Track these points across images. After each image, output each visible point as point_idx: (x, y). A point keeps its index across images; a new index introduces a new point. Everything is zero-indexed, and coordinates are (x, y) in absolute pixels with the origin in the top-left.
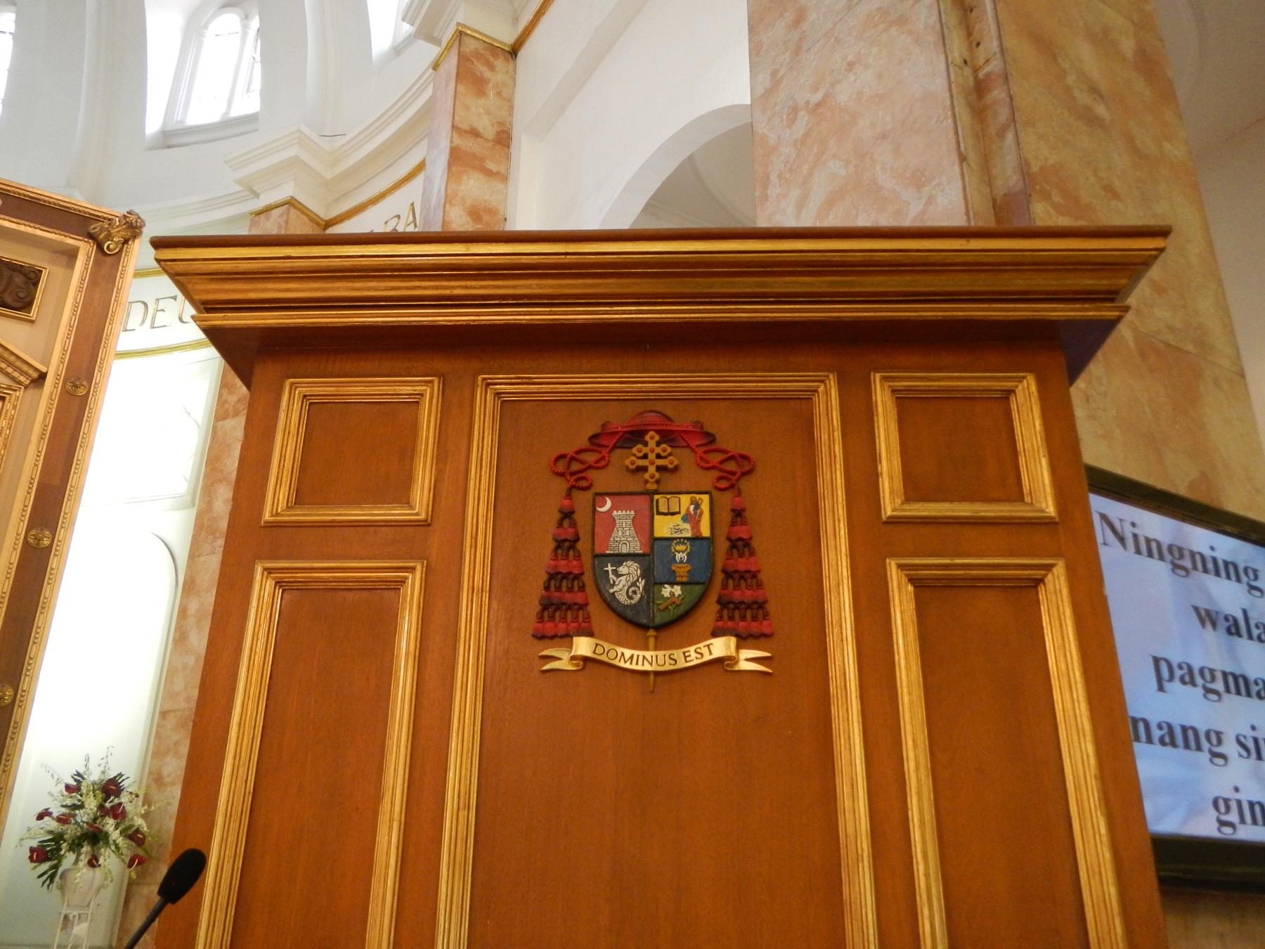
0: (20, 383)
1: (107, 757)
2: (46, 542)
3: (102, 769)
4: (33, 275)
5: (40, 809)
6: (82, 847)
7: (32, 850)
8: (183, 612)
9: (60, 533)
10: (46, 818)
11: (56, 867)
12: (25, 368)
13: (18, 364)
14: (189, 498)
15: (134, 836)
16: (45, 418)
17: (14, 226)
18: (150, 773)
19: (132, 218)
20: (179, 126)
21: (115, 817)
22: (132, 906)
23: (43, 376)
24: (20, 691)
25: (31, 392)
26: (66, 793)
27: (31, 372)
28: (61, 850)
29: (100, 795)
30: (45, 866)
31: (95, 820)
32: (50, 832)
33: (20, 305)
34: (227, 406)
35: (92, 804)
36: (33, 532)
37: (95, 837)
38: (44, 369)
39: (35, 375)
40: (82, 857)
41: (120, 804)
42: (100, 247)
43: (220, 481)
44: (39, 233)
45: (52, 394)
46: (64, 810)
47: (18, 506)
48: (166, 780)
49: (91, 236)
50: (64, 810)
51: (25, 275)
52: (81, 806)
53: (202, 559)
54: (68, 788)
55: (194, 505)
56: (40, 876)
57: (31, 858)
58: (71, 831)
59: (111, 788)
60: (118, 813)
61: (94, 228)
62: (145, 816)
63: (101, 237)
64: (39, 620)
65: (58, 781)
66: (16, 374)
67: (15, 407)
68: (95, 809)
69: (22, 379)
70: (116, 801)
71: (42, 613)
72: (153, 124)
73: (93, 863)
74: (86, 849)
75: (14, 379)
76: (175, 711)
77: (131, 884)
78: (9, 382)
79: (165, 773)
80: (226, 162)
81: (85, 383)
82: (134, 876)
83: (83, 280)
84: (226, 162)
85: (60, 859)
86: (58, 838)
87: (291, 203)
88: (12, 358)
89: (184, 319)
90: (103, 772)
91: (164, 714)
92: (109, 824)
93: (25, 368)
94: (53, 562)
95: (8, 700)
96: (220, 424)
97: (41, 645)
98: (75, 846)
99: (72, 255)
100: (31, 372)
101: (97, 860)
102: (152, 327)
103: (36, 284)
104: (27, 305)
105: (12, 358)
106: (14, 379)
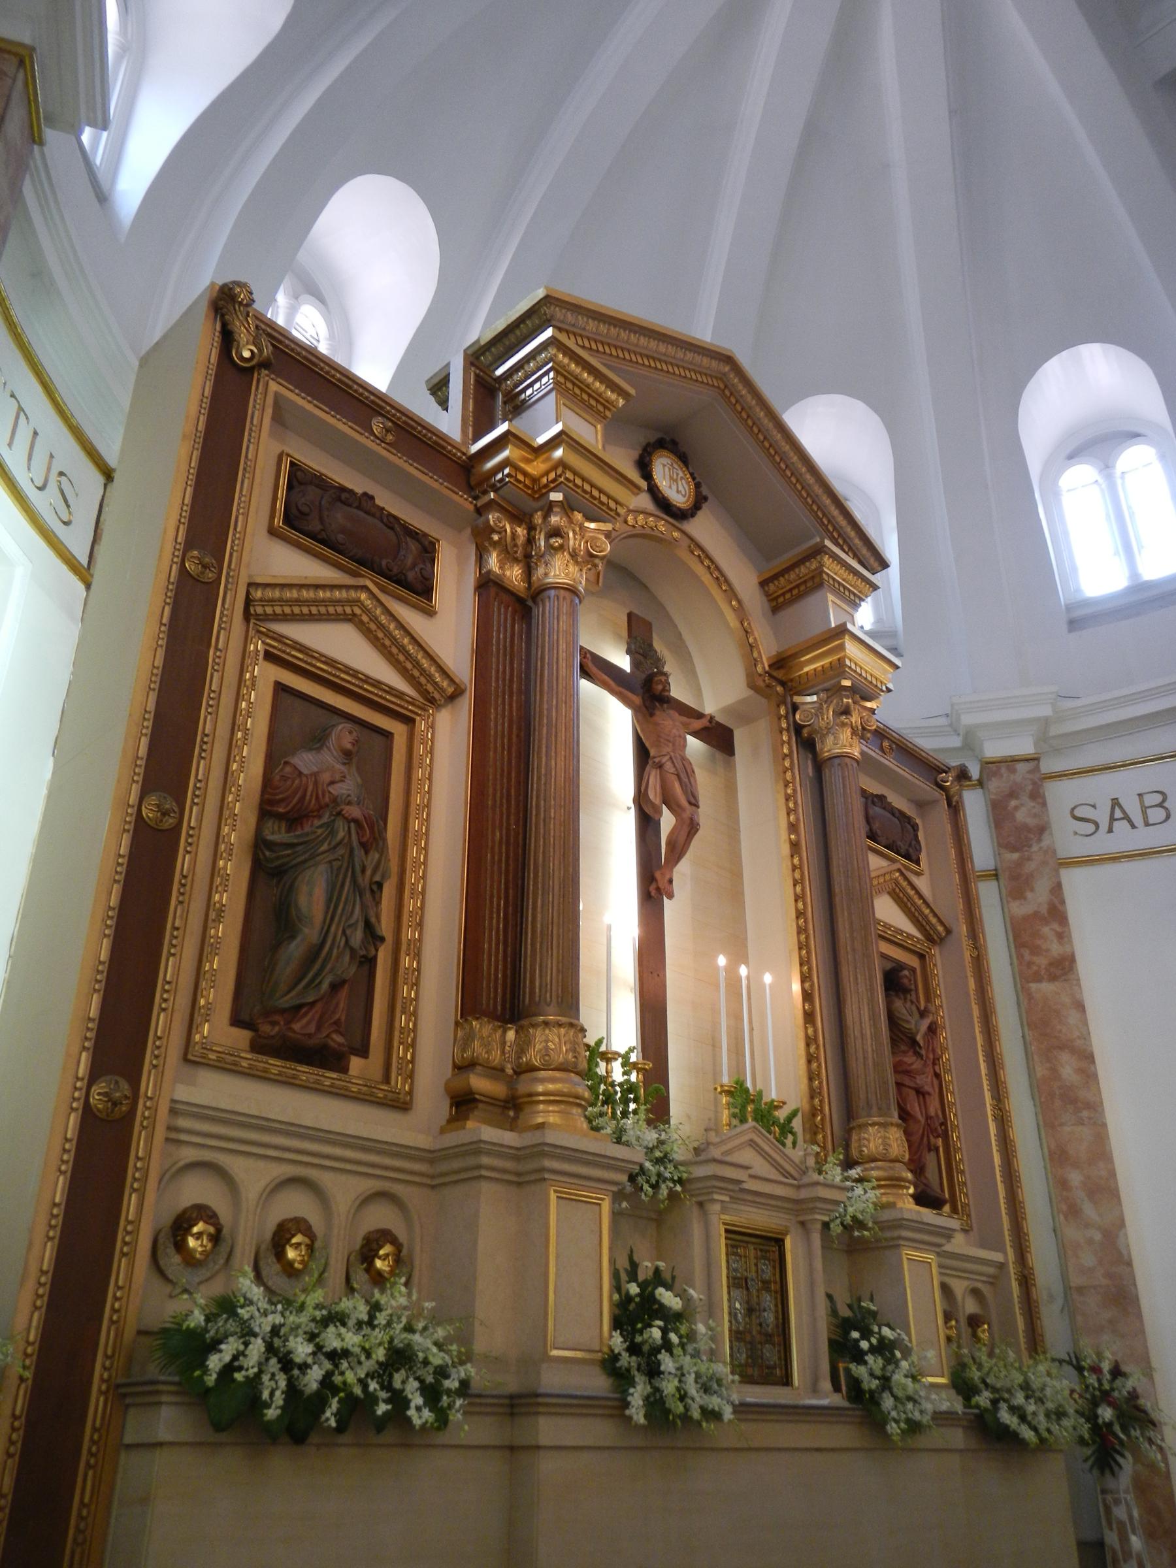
53: (1067, 1129)
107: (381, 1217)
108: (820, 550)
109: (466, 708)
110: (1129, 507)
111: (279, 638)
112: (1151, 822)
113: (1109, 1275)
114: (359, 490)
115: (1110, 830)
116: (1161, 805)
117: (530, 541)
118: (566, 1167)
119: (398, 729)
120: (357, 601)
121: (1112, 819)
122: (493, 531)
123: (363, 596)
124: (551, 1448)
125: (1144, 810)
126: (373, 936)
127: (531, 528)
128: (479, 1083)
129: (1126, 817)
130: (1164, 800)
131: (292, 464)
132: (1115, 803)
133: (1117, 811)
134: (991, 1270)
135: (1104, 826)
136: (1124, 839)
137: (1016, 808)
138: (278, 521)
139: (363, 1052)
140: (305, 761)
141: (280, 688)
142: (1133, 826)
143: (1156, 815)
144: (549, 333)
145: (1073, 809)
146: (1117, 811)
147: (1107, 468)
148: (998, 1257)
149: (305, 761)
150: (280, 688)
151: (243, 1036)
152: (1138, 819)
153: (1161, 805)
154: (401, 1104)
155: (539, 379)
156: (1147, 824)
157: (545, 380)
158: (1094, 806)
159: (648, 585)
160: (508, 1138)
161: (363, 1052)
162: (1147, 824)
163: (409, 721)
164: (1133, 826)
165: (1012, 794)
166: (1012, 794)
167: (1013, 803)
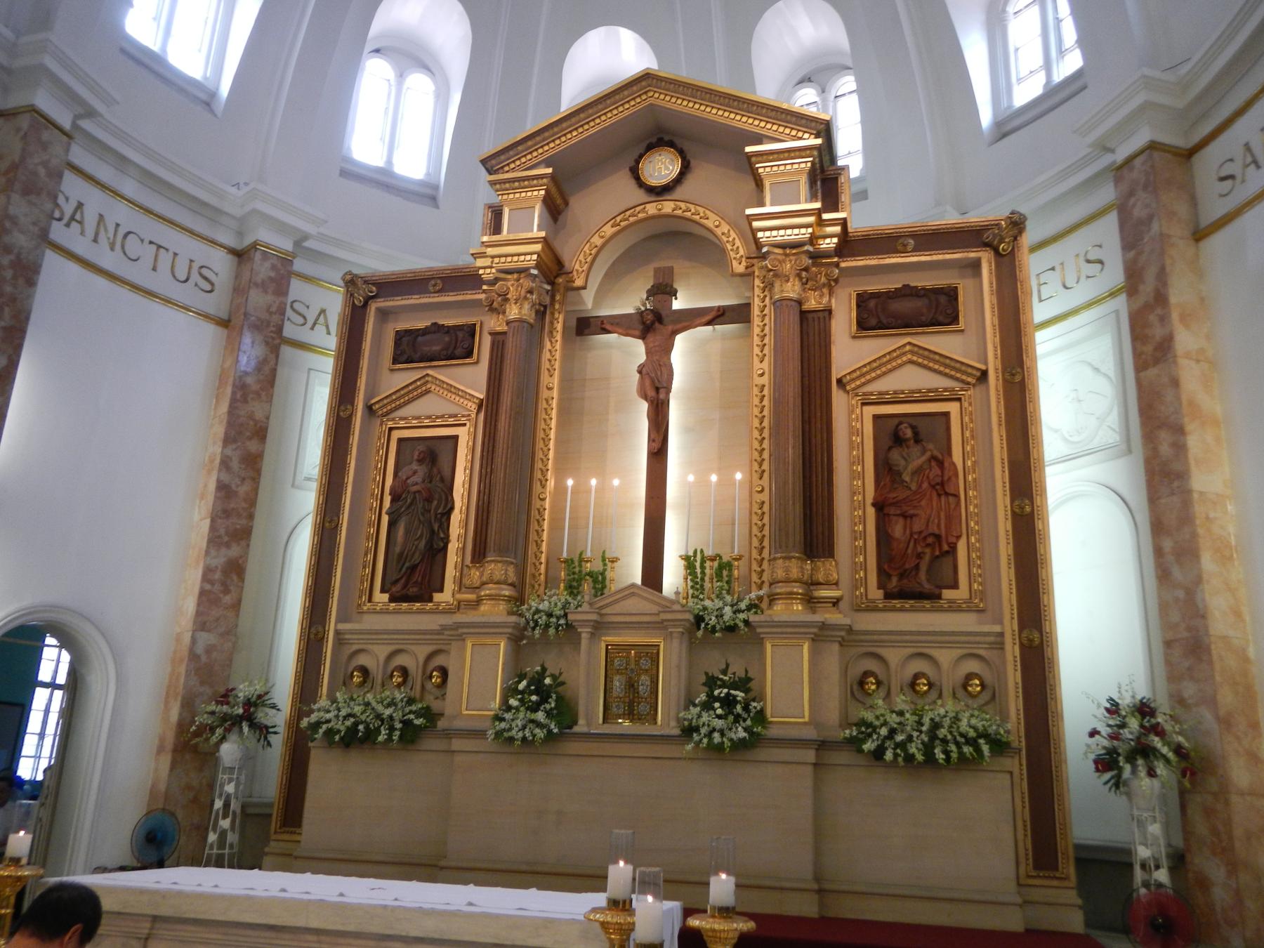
0: (968, 383)
1: (1131, 683)
2: (1028, 509)
3: (1131, 693)
4: (952, 293)
5: (1089, 729)
6: (1136, 759)
7: (1096, 762)
8: (1158, 552)
9: (1038, 501)
10: (1097, 737)
11: (1119, 776)
12: (970, 370)
13: (963, 368)
14: (1124, 447)
15: (1178, 750)
16: (998, 407)
17: (928, 258)
18: (1171, 696)
19: (1016, 217)
20: (1008, 113)
21: (1157, 734)
22: (1189, 812)
23: (984, 374)
24: (1044, 634)
25: (978, 389)
26: (1107, 715)
27: (974, 372)
28: (1118, 762)
29: (1139, 717)
30: (1108, 776)
31: (1138, 738)
32: (1104, 748)
33: (950, 320)
34: (1144, 357)
35: (1134, 724)
36: (1017, 503)
37: (1142, 751)
38: (983, 367)
39: (978, 374)
40: (1140, 768)
41: (1158, 724)
42: (996, 251)
43: (1159, 427)
44: (948, 257)
45: (997, 386)
46: (1109, 730)
47: (999, 485)
48: (1190, 701)
49: (987, 245)
50: (1109, 730)
51: (945, 294)
52: (1123, 726)
53: (1163, 501)
54: (1108, 710)
55: (1130, 451)
56: (1106, 783)
57: (1097, 770)
58: (1123, 748)
59: (1144, 709)
60: (1157, 730)
61: (987, 237)
62: (1180, 733)
63: (995, 242)
64: (1042, 574)
65: (1099, 706)
66: (964, 377)
67: (970, 404)
68: (1138, 728)
69: (969, 379)
70: (1153, 721)
71: (1042, 568)
72: (986, 117)
73: (1151, 773)
74: (1140, 762)
75: (963, 381)
76: (1176, 640)
77: (1182, 793)
78: (961, 385)
79: (1186, 695)
80: (1075, 132)
81: (1019, 370)
82: (1187, 784)
83: (991, 283)
84: (1075, 132)
85: (1120, 769)
86: (1112, 752)
87: (1153, 146)
88: (958, 365)
89: (1068, 286)
90: (1133, 697)
91: (1168, 644)
92: (1156, 742)
93: (970, 370)
94: (1039, 525)
95: (1037, 641)
96: (1142, 374)
97: (1049, 592)
98: (1131, 759)
99: (975, 266)
100: (974, 372)
101: (1155, 772)
102: (1041, 301)
103: (956, 299)
104: (954, 319)
105: (958, 365)
106: (963, 381)
108: (749, 156)
113: (1189, 629)
118: (472, 630)
120: (427, 382)
123: (430, 379)
124: (459, 751)
132: (1247, 147)
134: (992, 639)
137: (1134, 205)
148: (997, 629)
158: (1231, 160)
159: (688, 231)
161: (441, 590)
165: (1131, 193)
166: (1131, 193)
167: (1132, 200)
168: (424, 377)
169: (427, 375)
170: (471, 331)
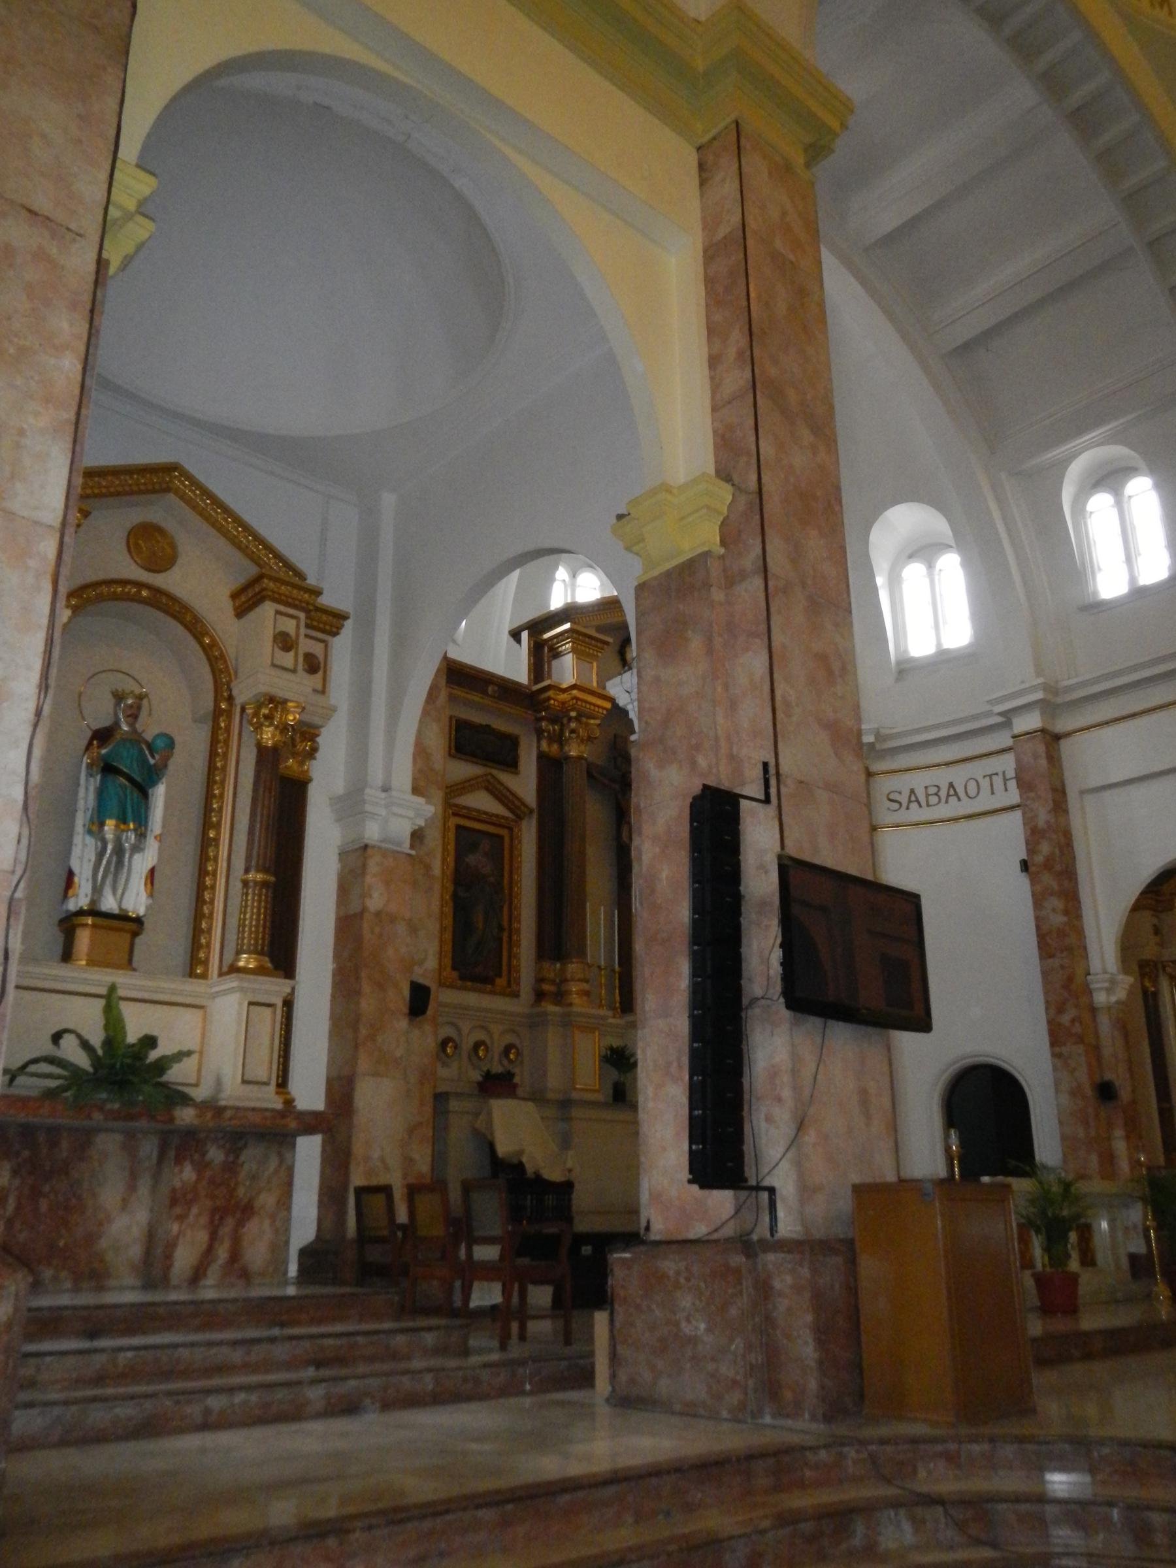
107: (509, 1039)
109: (535, 822)
110: (941, 595)
111: (456, 806)
112: (930, 803)
114: (484, 723)
115: (908, 808)
116: (936, 794)
117: (562, 731)
119: (504, 832)
121: (910, 801)
122: (544, 731)
125: (927, 795)
126: (501, 929)
127: (562, 725)
128: (546, 987)
129: (918, 801)
130: (939, 791)
131: (456, 720)
132: (912, 791)
133: (913, 796)
135: (905, 805)
136: (916, 814)
138: (453, 751)
139: (500, 976)
140: (471, 859)
141: (459, 827)
142: (920, 806)
143: (933, 800)
144: (567, 626)
145: (888, 794)
146: (913, 796)
147: (930, 566)
149: (471, 859)
150: (459, 827)
151: (455, 974)
152: (923, 803)
153: (936, 794)
154: (516, 995)
155: (564, 644)
156: (928, 805)
157: (567, 646)
158: (900, 793)
160: (557, 1009)
162: (928, 805)
163: (510, 829)
164: (920, 806)
168: (486, 775)
169: (491, 774)
170: (512, 742)
